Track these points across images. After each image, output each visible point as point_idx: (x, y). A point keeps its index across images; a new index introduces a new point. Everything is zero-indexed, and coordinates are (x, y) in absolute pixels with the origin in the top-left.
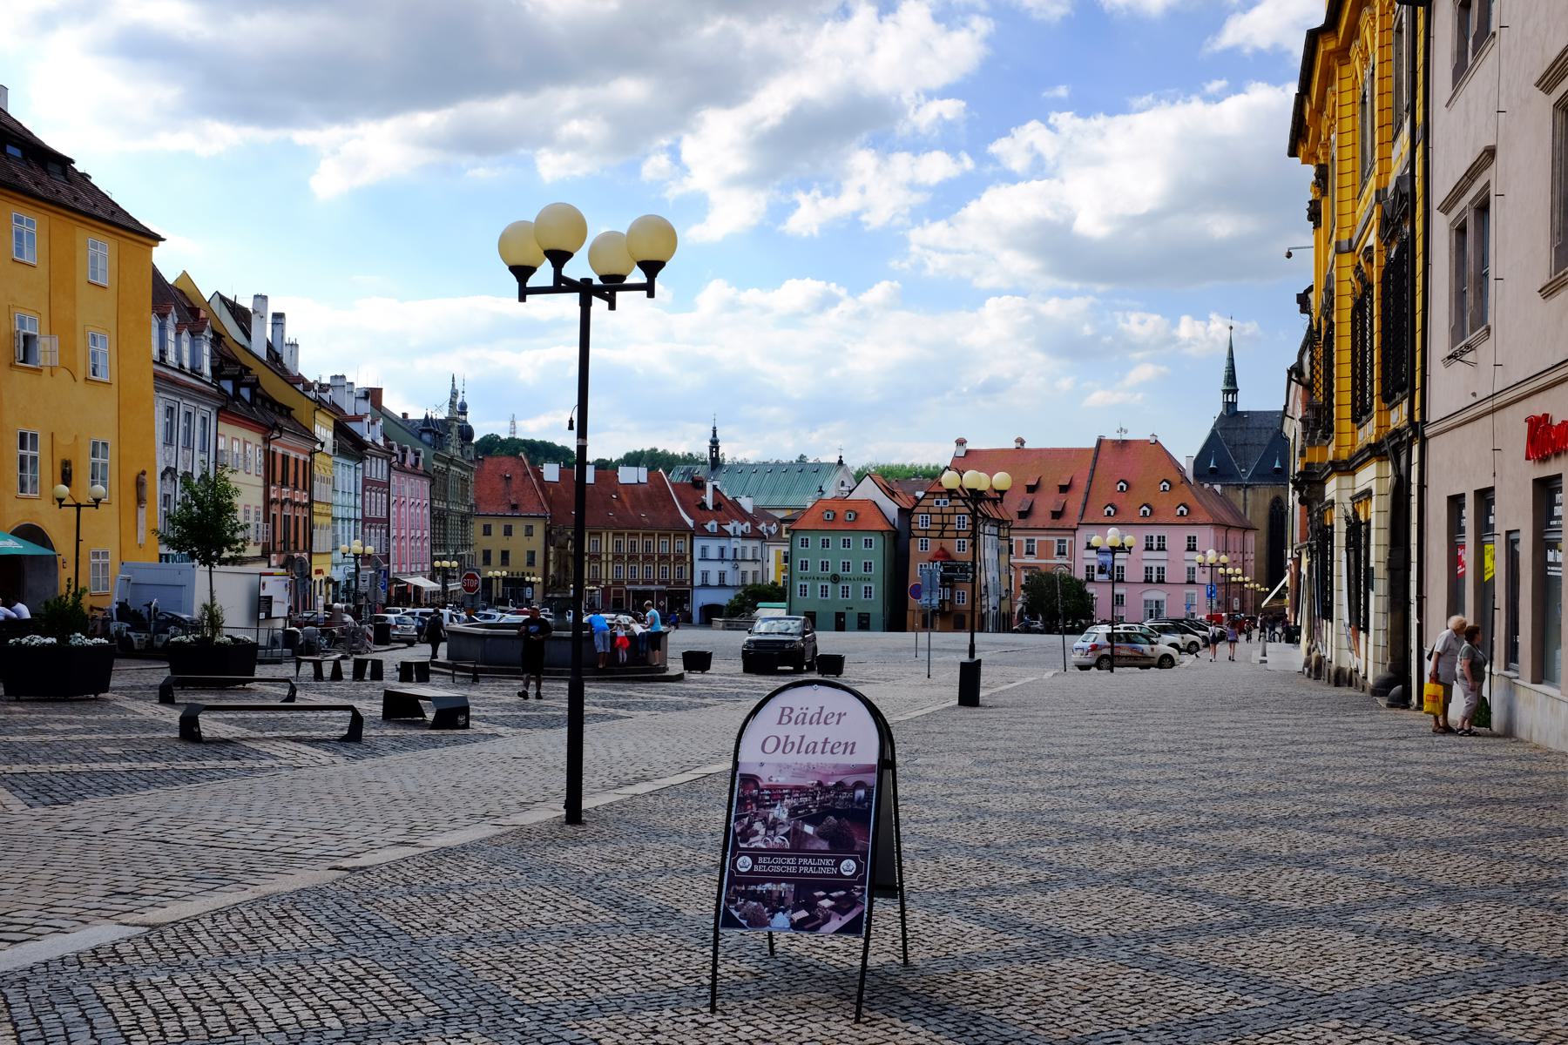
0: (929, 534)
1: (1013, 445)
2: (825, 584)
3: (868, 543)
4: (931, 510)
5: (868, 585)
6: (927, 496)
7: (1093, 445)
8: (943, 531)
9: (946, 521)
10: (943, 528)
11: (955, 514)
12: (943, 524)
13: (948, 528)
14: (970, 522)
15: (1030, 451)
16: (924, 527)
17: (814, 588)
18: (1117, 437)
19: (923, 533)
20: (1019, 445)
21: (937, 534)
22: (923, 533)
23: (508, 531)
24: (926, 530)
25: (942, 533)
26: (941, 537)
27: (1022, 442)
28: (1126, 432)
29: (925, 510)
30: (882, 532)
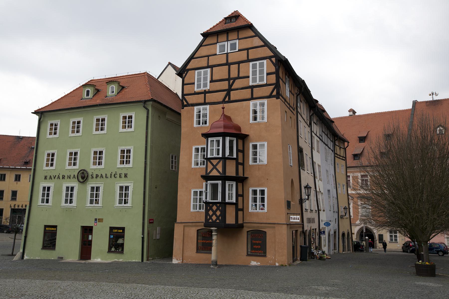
0: (210, 98)
1: (347, 114)
2: (70, 185)
3: (127, 121)
4: (213, 61)
5: (124, 185)
6: (207, 42)
7: (410, 107)
8: (229, 91)
9: (234, 74)
10: (230, 86)
11: (248, 61)
12: (228, 79)
13: (238, 84)
14: (273, 69)
15: (360, 116)
16: (202, 89)
17: (58, 191)
18: (430, 99)
19: (201, 98)
20: (351, 113)
21: (220, 96)
22: (201, 98)
23: (18, 178)
24: (205, 92)
25: (228, 94)
26: (227, 100)
27: (354, 112)
28: (436, 95)
29: (203, 62)
30: (145, 102)
